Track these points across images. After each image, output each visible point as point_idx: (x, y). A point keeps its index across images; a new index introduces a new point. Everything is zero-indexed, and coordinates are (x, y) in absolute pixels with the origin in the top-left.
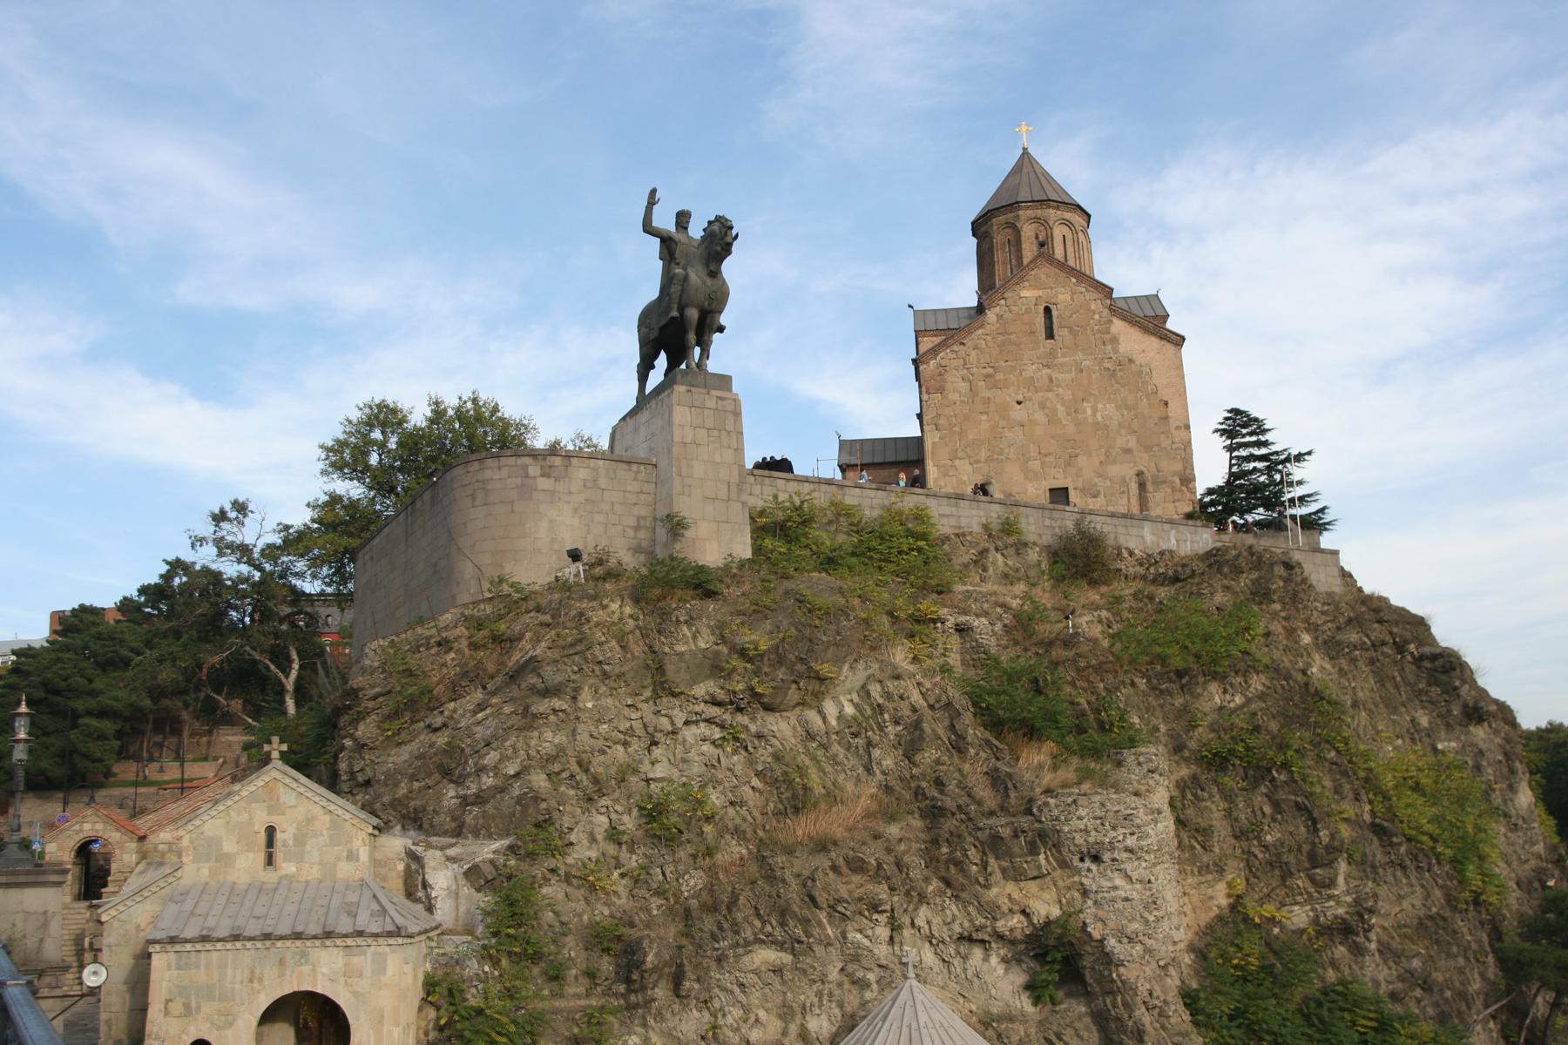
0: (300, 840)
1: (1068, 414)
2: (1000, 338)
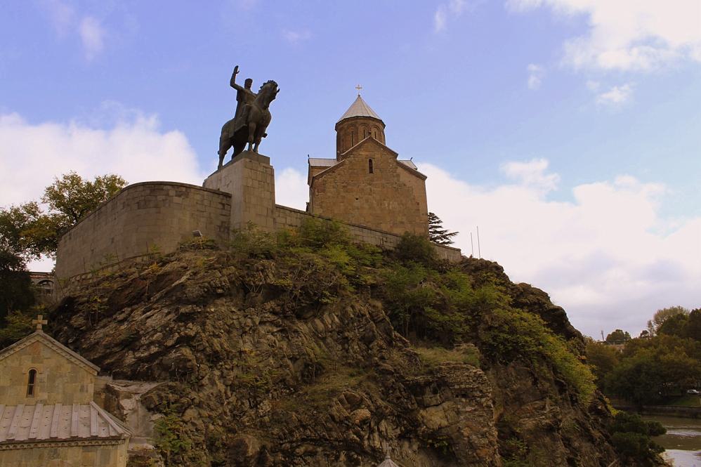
0: (52, 378)
1: (378, 205)
2: (350, 171)
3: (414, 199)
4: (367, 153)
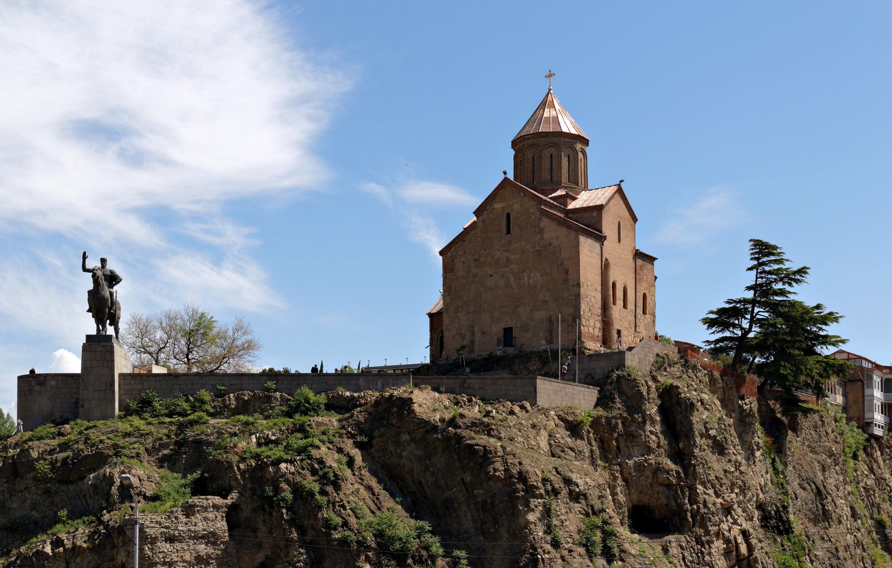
3: (562, 264)
4: (503, 204)
